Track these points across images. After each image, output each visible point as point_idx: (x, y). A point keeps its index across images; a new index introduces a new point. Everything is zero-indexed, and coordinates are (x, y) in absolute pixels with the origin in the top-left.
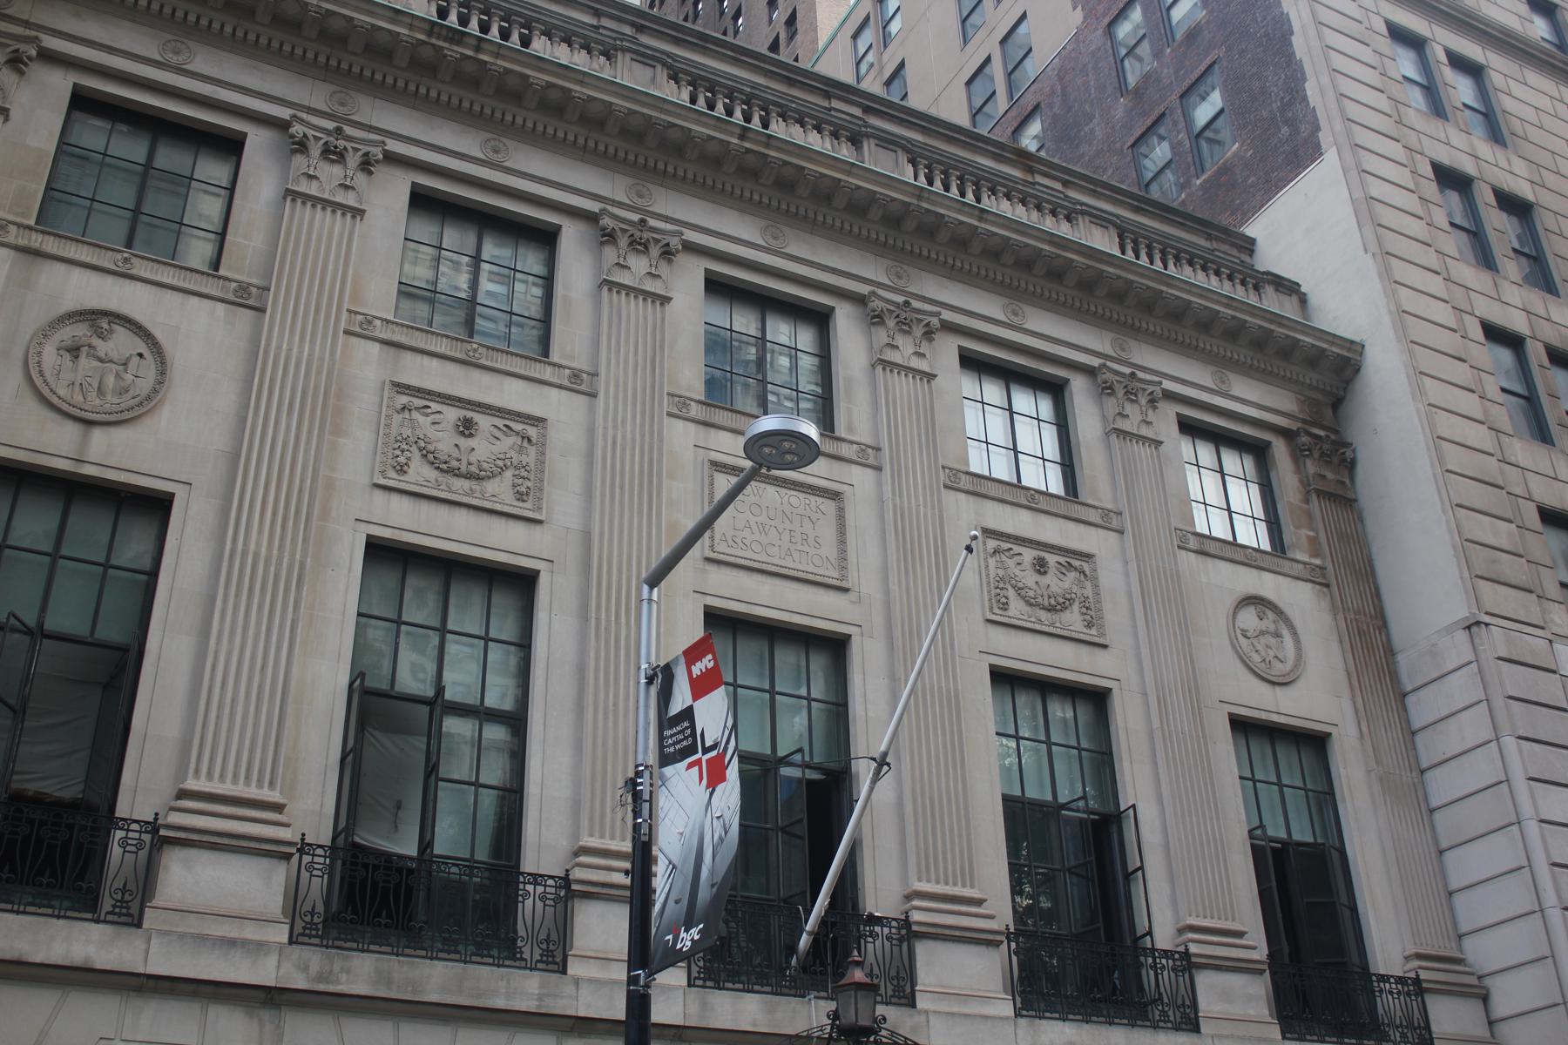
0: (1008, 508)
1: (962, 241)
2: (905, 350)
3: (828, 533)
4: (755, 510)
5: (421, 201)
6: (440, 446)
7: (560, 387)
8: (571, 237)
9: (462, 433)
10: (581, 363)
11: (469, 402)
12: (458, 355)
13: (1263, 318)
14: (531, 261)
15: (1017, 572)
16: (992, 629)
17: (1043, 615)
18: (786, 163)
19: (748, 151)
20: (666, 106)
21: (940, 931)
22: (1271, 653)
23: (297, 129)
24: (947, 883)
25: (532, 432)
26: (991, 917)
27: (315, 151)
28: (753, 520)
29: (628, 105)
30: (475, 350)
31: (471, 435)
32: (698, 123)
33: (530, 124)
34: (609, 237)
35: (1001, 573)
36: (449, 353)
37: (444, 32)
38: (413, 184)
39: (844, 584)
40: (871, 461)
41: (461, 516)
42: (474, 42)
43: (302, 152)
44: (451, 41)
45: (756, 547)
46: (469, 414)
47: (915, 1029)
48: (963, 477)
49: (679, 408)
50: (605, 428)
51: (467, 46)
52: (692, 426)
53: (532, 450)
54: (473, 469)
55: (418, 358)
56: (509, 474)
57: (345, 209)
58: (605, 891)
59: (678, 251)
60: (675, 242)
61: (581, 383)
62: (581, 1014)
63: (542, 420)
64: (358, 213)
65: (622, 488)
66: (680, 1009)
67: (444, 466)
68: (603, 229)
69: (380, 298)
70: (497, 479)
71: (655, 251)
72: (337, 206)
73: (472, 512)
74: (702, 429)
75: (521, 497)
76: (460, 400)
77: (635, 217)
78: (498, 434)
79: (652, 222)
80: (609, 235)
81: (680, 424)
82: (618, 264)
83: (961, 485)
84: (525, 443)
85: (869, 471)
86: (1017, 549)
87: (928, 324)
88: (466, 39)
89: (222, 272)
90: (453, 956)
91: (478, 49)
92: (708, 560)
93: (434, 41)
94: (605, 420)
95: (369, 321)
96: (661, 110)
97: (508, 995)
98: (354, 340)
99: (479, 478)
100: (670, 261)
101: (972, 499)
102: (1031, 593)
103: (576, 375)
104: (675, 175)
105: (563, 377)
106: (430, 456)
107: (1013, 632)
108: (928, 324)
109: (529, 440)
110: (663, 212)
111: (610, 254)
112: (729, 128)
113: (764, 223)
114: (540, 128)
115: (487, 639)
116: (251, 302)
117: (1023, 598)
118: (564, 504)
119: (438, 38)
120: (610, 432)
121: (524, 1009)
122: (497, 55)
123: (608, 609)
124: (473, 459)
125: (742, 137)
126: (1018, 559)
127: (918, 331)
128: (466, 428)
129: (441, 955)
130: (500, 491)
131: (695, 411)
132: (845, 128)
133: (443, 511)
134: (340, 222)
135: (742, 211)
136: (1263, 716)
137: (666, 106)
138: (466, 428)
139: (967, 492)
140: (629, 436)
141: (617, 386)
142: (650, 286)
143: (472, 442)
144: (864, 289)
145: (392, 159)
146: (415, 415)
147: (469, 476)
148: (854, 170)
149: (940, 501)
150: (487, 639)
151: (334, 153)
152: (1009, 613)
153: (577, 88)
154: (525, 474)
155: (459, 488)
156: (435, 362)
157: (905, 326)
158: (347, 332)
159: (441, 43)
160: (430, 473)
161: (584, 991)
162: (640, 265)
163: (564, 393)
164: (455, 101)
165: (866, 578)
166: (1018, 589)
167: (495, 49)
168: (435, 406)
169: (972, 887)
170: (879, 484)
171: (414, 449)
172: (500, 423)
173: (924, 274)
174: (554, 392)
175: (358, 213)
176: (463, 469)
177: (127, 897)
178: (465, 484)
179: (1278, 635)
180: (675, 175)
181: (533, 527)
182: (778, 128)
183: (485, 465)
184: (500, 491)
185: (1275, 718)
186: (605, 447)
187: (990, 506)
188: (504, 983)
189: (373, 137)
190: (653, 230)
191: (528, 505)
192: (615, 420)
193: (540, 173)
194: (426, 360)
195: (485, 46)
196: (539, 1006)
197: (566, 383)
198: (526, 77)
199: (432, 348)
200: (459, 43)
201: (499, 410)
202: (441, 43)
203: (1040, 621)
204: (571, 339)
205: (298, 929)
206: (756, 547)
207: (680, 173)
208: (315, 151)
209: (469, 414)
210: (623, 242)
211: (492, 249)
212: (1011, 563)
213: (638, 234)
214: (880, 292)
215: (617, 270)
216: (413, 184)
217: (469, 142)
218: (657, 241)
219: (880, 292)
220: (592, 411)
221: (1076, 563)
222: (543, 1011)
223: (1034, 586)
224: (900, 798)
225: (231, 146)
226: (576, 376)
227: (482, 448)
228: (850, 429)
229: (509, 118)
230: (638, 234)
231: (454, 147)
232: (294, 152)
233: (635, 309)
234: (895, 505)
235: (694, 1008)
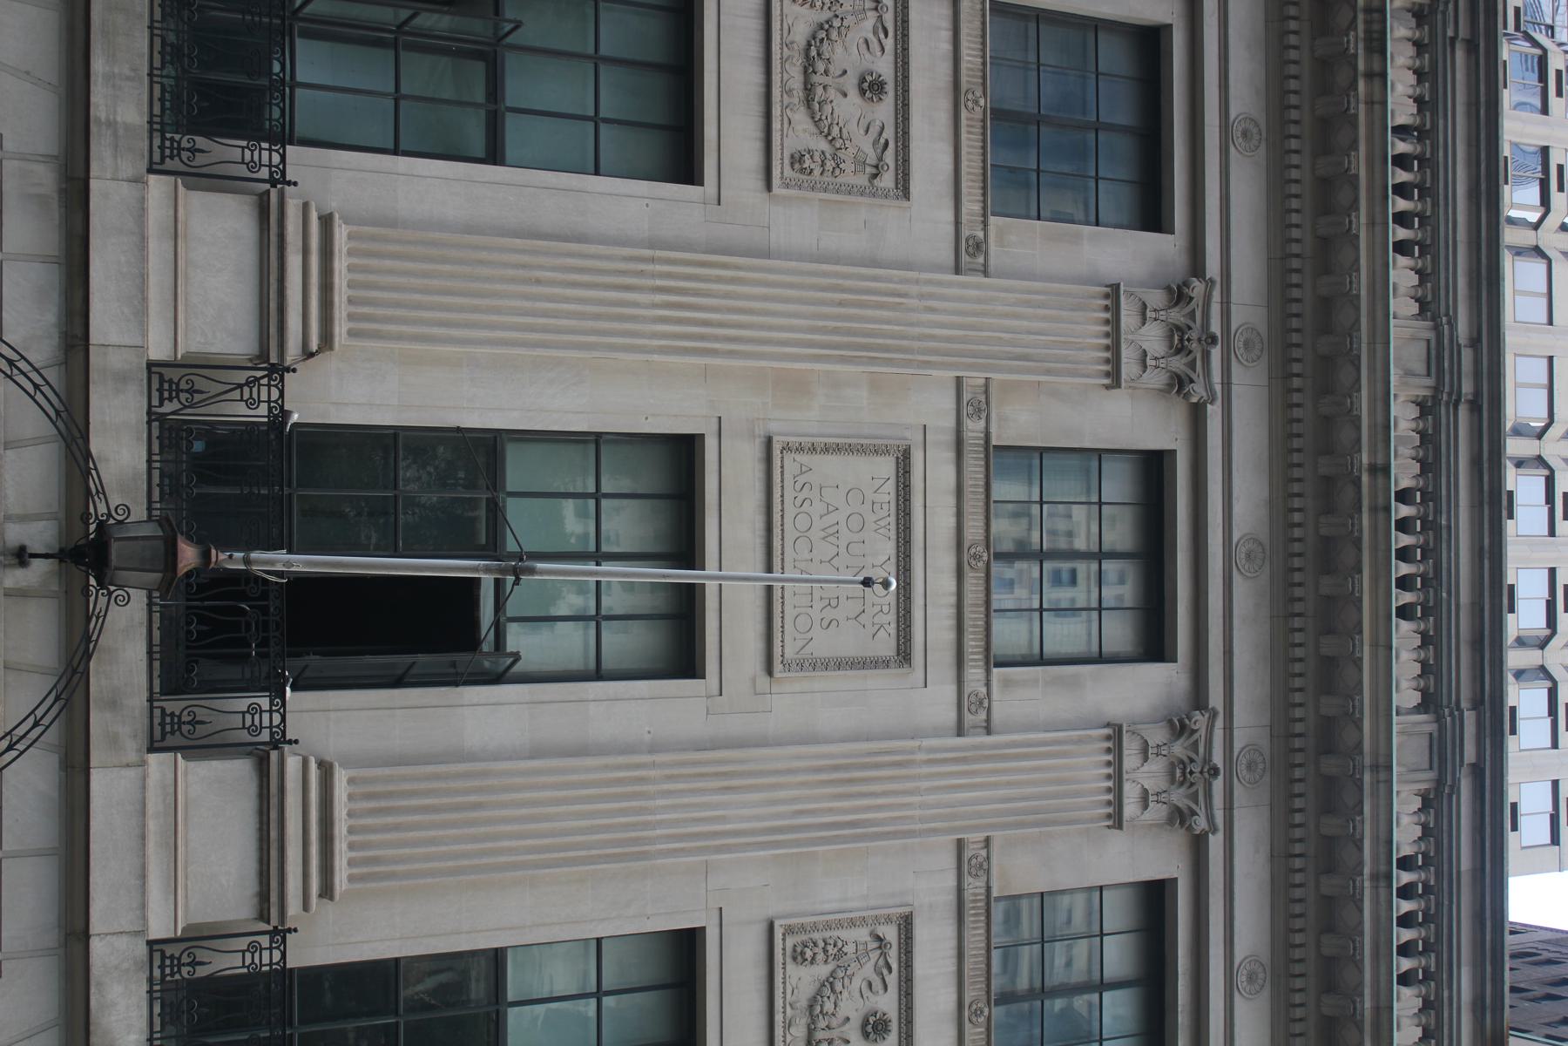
0: (950, 966)
1: (1330, 251)
2: (1144, 775)
3: (847, 642)
4: (855, 522)
5: (1153, 468)
6: (839, 49)
7: (957, 223)
8: (1163, 250)
9: (863, 80)
10: (996, 254)
11: (906, 91)
12: (964, 79)
14: (1119, 632)
15: (857, 982)
16: (759, 932)
18: (1357, 543)
19: (1357, 483)
20: (1379, 347)
21: (274, 801)
23: (1198, 288)
24: (351, 831)
25: (887, 180)
26: (306, 907)
27: (1177, 316)
28: (840, 516)
29: (1363, 293)
30: (976, 102)
31: (863, 92)
32: (1372, 400)
33: (1294, 174)
34: (1178, 296)
35: (850, 949)
36: (964, 65)
37: (1376, 27)
38: (1170, 26)
39: (777, 666)
40: (969, 718)
41: (754, 75)
42: (1376, 67)
43: (1171, 300)
44: (1369, 39)
45: (803, 522)
46: (890, 88)
47: (113, 741)
48: (981, 883)
49: (971, 402)
50: (917, 282)
51: (1368, 60)
52: (950, 422)
53: (862, 180)
54: (819, 90)
55: (946, 23)
56: (823, 145)
57: (1115, 362)
58: (274, 238)
59: (1187, 396)
60: (1198, 391)
61: (969, 253)
62: (93, 184)
63: (906, 194)
64: (1114, 378)
65: (841, 304)
66: (114, 339)
67: (813, 53)
68: (1186, 284)
69: (1019, 423)
70: (813, 128)
71: (1178, 364)
72: (1115, 348)
73: (762, 90)
74: (950, 437)
75: (797, 159)
76: (906, 77)
77: (1218, 759)
78: (874, 130)
79: (1218, 785)
80: (1183, 726)
81: (949, 403)
82: (1144, 306)
83: (968, 880)
84: (869, 170)
85: (953, 715)
86: (892, 980)
87: (1194, 813)
88: (1376, 57)
89: (992, 220)
90: (157, 57)
91: (1369, 75)
92: (769, 442)
93: (1361, 17)
94: (929, 282)
95: (983, 408)
96: (1372, 343)
97: (109, 77)
98: (952, 393)
99: (808, 102)
100: (1170, 821)
101: (951, 897)
102: (829, 1006)
103: (979, 247)
104: (1291, 391)
105: (971, 229)
106: (822, 34)
107: (762, 972)
108: (1194, 813)
109: (875, 176)
110: (1234, 380)
111: (1156, 298)
112: (1380, 446)
113: (1265, 957)
114: (1294, 189)
115: (596, 120)
116: (965, 258)
117: (819, 993)
118: (797, 221)
119: (1366, 22)
120: (914, 289)
121: (93, 99)
122: (1370, 103)
123: (669, 276)
124: (832, 93)
125: (1373, 469)
126: (877, 984)
127: (1178, 797)
128: (871, 87)
129: (158, 41)
130: (797, 132)
131: (974, 886)
132: (1438, 681)
133: (754, 50)
134: (1093, 356)
135: (1271, 502)
137: (1379, 347)
138: (871, 87)
139: (960, 890)
140: (914, 317)
141: (979, 301)
142: (1128, 355)
143: (853, 94)
144: (1216, 699)
145: (1197, 417)
146: (872, 16)
147: (808, 88)
148: (1382, 652)
149: (935, 831)
150: (596, 120)
151: (1181, 340)
152: (790, 966)
153: (1363, 220)
154: (830, 165)
155: (790, 75)
156: (946, 47)
157: (1180, 773)
158: (959, 380)
159: (1361, 27)
160: (800, 34)
161: (126, 189)
162: (1153, 338)
163: (951, 229)
164: (1293, 69)
165: (798, 704)
166: (829, 982)
167: (1377, 97)
168: (889, 43)
169: (351, 878)
170: (937, 732)
171: (827, 15)
172: (889, 134)
173: (1266, 811)
174: (948, 215)
175: (1114, 378)
176: (816, 79)
177: (185, 155)
178: (796, 82)
180: (1291, 391)
181: (761, 176)
182: (1405, 634)
183: (827, 109)
184: (797, 132)
186: (889, 280)
187: (950, 931)
188: (127, 72)
189: (1218, 388)
190: (1206, 356)
191: (788, 172)
192: (931, 296)
193: (1237, 614)
194: (946, 35)
195: (1377, 82)
196: (98, 120)
197: (965, 232)
198: (1354, 145)
199: (964, 44)
200: (1369, 50)
201: (906, 133)
202: (1361, 27)
203: (788, 1025)
204: (1024, 698)
205: (169, 373)
206: (803, 522)
207: (1296, 398)
208: (1177, 316)
209: (890, 88)
210: (1179, 749)
211: (1122, 585)
212: (868, 971)
213: (1194, 335)
214: (1219, 723)
215: (1137, 307)
216: (1170, 26)
217: (1246, 97)
218: (1192, 365)
219: (1219, 723)
220: (938, 268)
222: (93, 128)
223: (841, 1014)
224: (471, 757)
225: (1152, 217)
226: (978, 246)
227: (848, 108)
228: (1007, 683)
229: (1294, 144)
230: (1194, 335)
231: (1238, 497)
232: (1169, 289)
233: (1089, 330)
234: (912, 752)
235: (116, 361)
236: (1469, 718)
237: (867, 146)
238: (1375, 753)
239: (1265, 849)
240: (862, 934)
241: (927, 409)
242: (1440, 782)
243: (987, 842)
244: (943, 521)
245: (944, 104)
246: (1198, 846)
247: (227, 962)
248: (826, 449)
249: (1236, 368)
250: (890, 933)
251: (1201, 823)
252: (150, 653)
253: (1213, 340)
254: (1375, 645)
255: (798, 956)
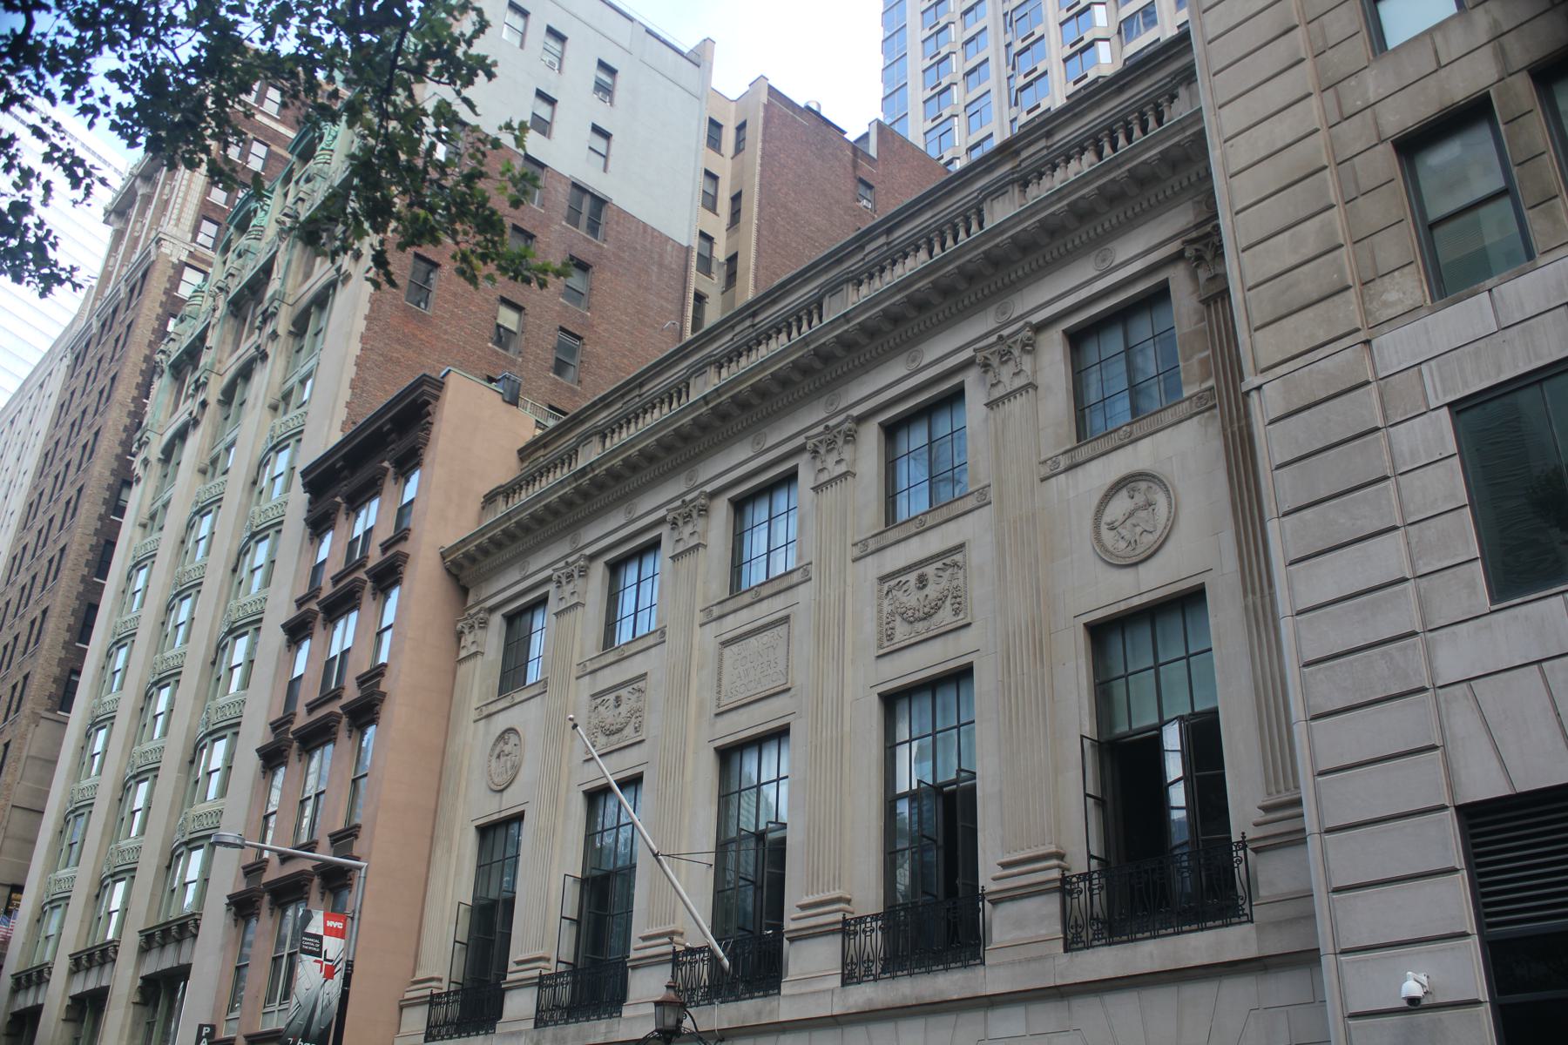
13: (1099, 177)
15: (904, 599)
17: (920, 626)
22: (1138, 530)
48: (871, 542)
86: (904, 579)
107: (895, 656)
136: (1123, 606)
139: (873, 553)
179: (1149, 504)
184: (629, 735)
185: (1136, 602)
221: (947, 561)
236: (869, 248)
237: (633, 698)
238: (801, 348)
239: (865, 378)
240: (886, 602)
241: (707, 638)
242: (847, 281)
243: (855, 545)
244: (744, 615)
245: (625, 664)
246: (1040, 328)
247: (873, 942)
248: (719, 686)
249: (1117, 262)
250: (886, 587)
251: (846, 426)
252: (1178, 933)
253: (827, 427)
254: (765, 369)
255: (890, 637)
